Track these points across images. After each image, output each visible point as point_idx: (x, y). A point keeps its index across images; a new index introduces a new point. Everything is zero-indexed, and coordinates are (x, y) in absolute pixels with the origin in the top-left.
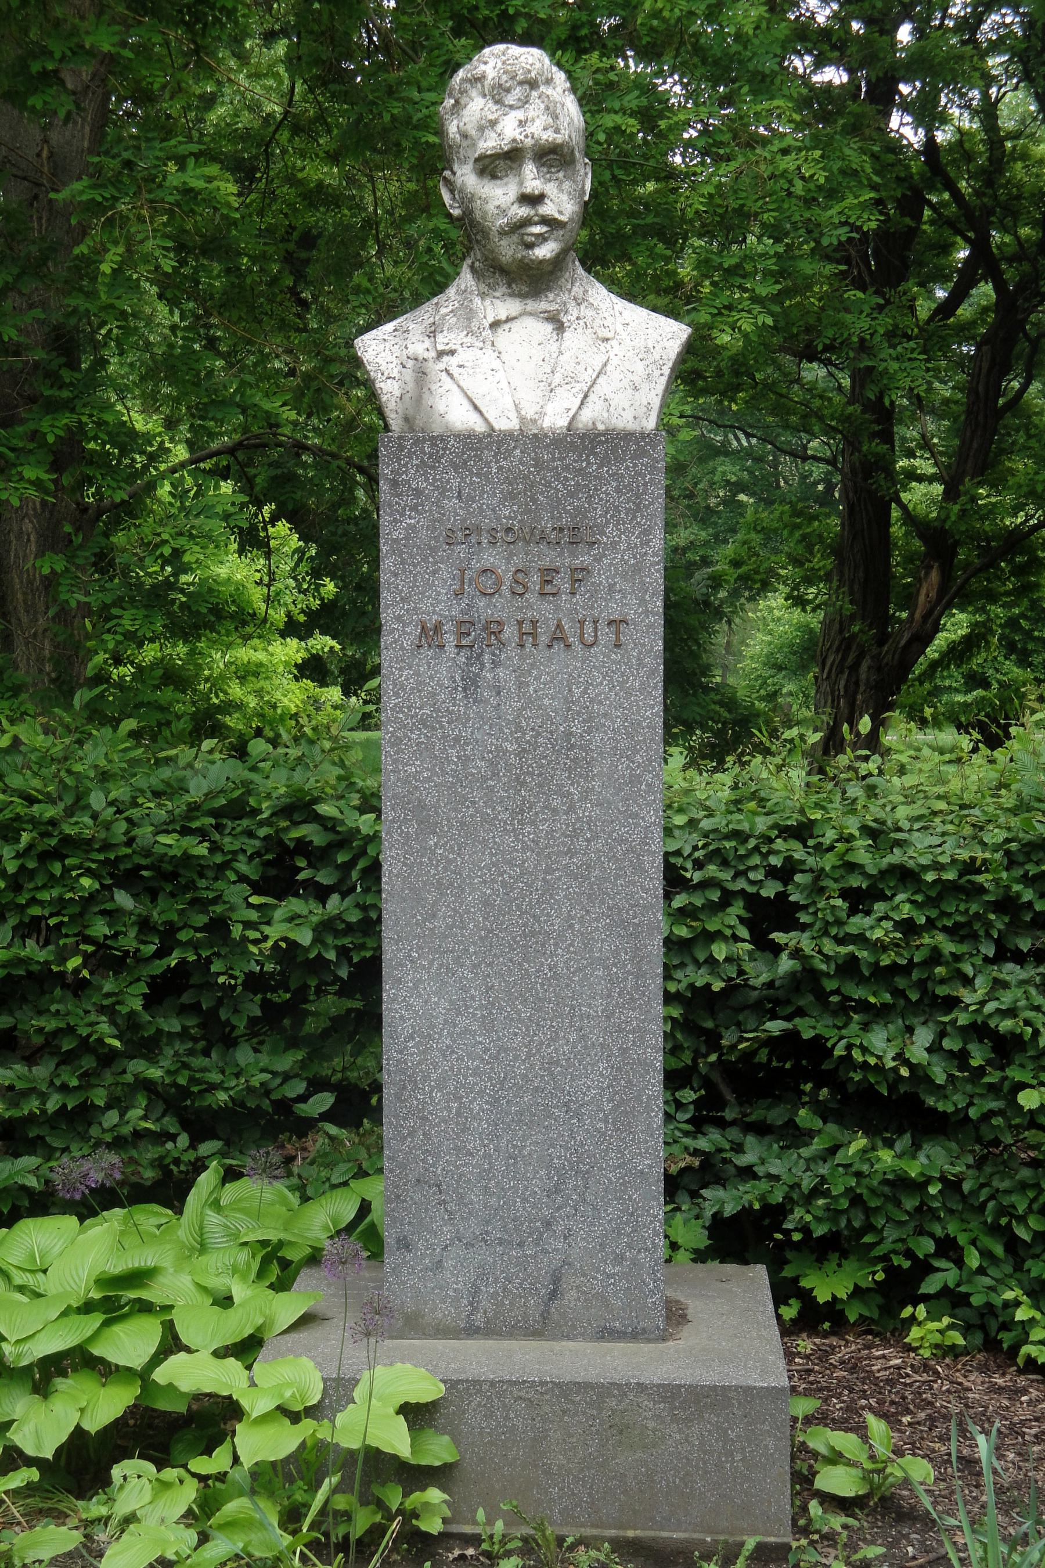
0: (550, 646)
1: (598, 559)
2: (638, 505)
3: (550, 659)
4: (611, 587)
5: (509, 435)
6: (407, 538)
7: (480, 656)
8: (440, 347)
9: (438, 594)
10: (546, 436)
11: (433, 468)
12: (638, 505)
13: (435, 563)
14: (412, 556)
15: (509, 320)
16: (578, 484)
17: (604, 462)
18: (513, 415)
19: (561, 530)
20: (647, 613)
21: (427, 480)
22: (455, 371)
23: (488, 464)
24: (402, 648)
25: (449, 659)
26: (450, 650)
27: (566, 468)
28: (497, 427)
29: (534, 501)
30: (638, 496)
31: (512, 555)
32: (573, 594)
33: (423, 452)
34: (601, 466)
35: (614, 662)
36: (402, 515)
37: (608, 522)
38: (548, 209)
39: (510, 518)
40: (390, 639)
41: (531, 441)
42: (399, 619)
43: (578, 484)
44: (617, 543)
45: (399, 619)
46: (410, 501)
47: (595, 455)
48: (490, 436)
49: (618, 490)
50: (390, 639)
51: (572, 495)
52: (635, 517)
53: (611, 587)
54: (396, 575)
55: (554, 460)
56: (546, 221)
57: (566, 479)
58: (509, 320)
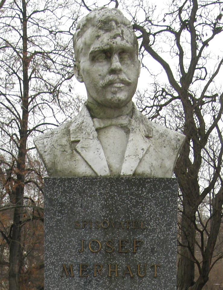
0: (123, 278)
1: (146, 236)
2: (165, 212)
3: (123, 283)
4: (153, 249)
5: (105, 178)
6: (57, 226)
7: (90, 281)
8: (72, 139)
9: (71, 252)
10: (122, 178)
11: (70, 193)
12: (165, 212)
13: (70, 237)
14: (59, 234)
15: (105, 128)
16: (137, 201)
17: (150, 191)
18: (107, 169)
19: (129, 223)
20: (169, 262)
21: (66, 198)
22: (79, 150)
23: (95, 192)
24: (54, 277)
25: (76, 283)
26: (77, 279)
27: (132, 194)
28: (99, 175)
29: (117, 209)
30: (165, 207)
31: (106, 234)
32: (135, 253)
33: (64, 185)
34: (148, 193)
35: (153, 284)
36: (55, 214)
37: (151, 219)
38: (123, 76)
39: (104, 216)
40: (48, 273)
41: (115, 181)
42: (53, 263)
43: (137, 201)
44: (156, 229)
45: (53, 263)
46: (58, 208)
47: (146, 188)
48: (96, 178)
49: (156, 204)
50: (48, 273)
51: (135, 206)
52: (164, 217)
53: (153, 249)
54: (51, 243)
55: (126, 190)
56: (122, 81)
57: (131, 198)
58: (105, 128)
